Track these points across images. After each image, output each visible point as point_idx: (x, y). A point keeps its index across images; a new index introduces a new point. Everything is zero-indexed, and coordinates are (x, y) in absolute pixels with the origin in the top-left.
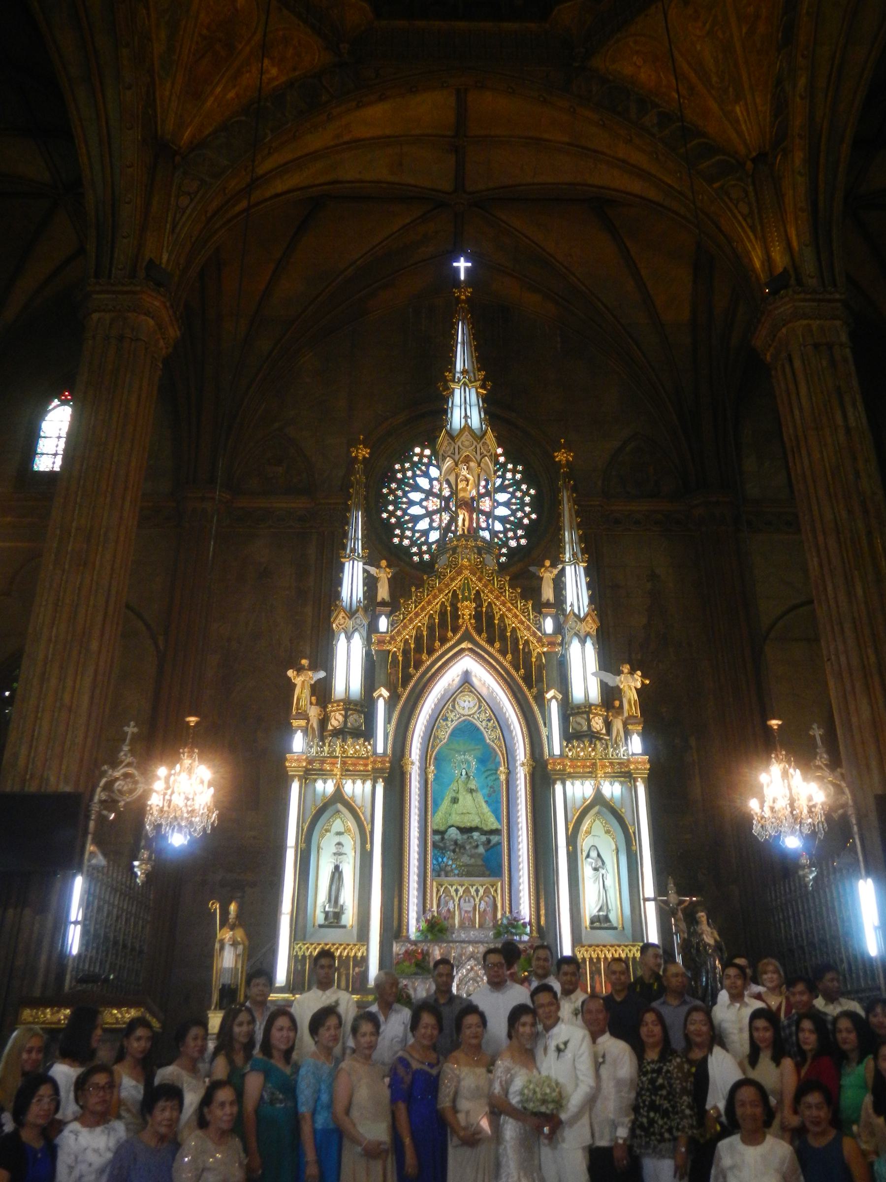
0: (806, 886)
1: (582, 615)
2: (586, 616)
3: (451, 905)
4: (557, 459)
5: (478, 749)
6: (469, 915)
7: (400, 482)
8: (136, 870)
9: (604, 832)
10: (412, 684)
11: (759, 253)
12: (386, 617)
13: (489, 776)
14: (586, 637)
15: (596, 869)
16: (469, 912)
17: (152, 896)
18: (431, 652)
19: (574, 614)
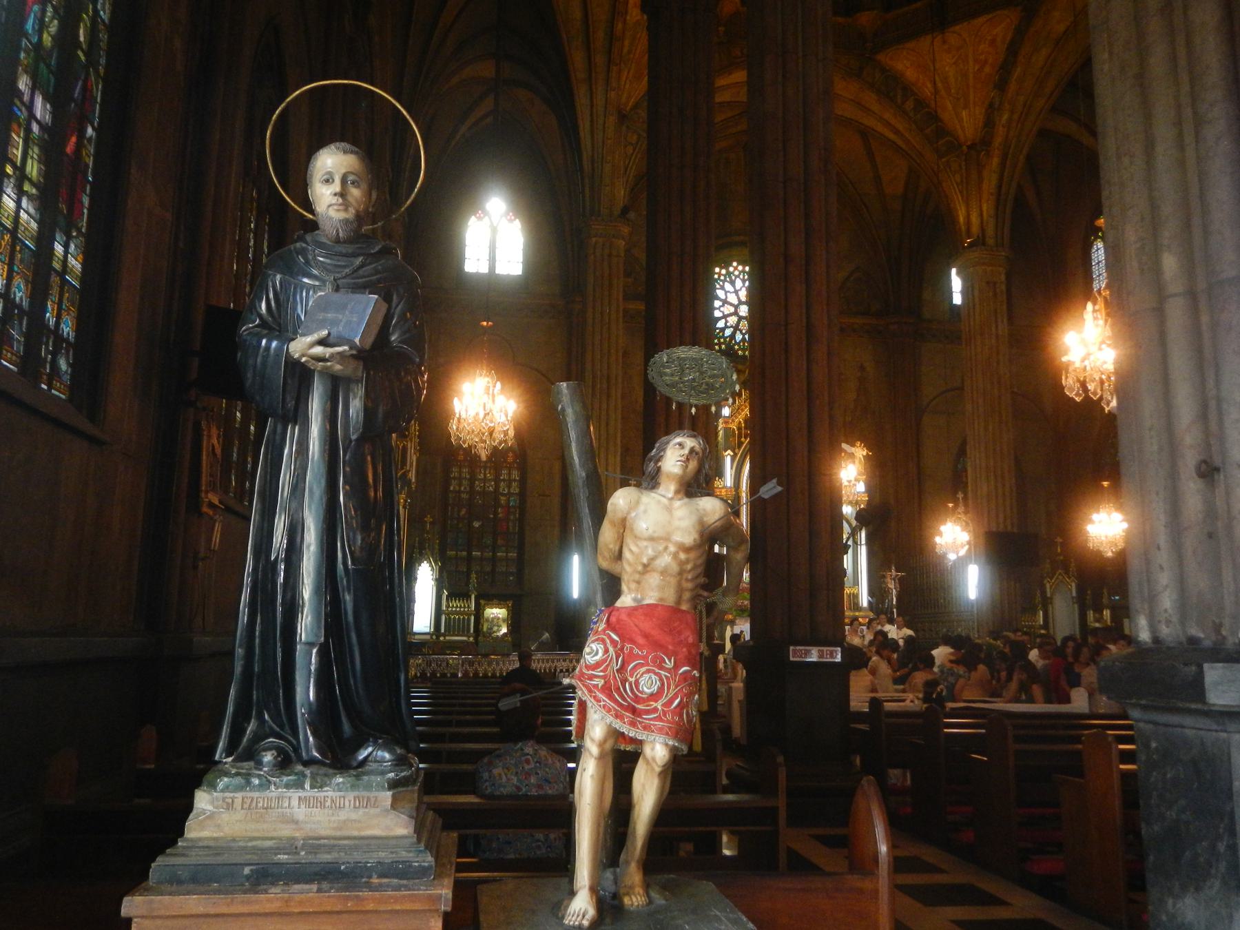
11: (964, 212)
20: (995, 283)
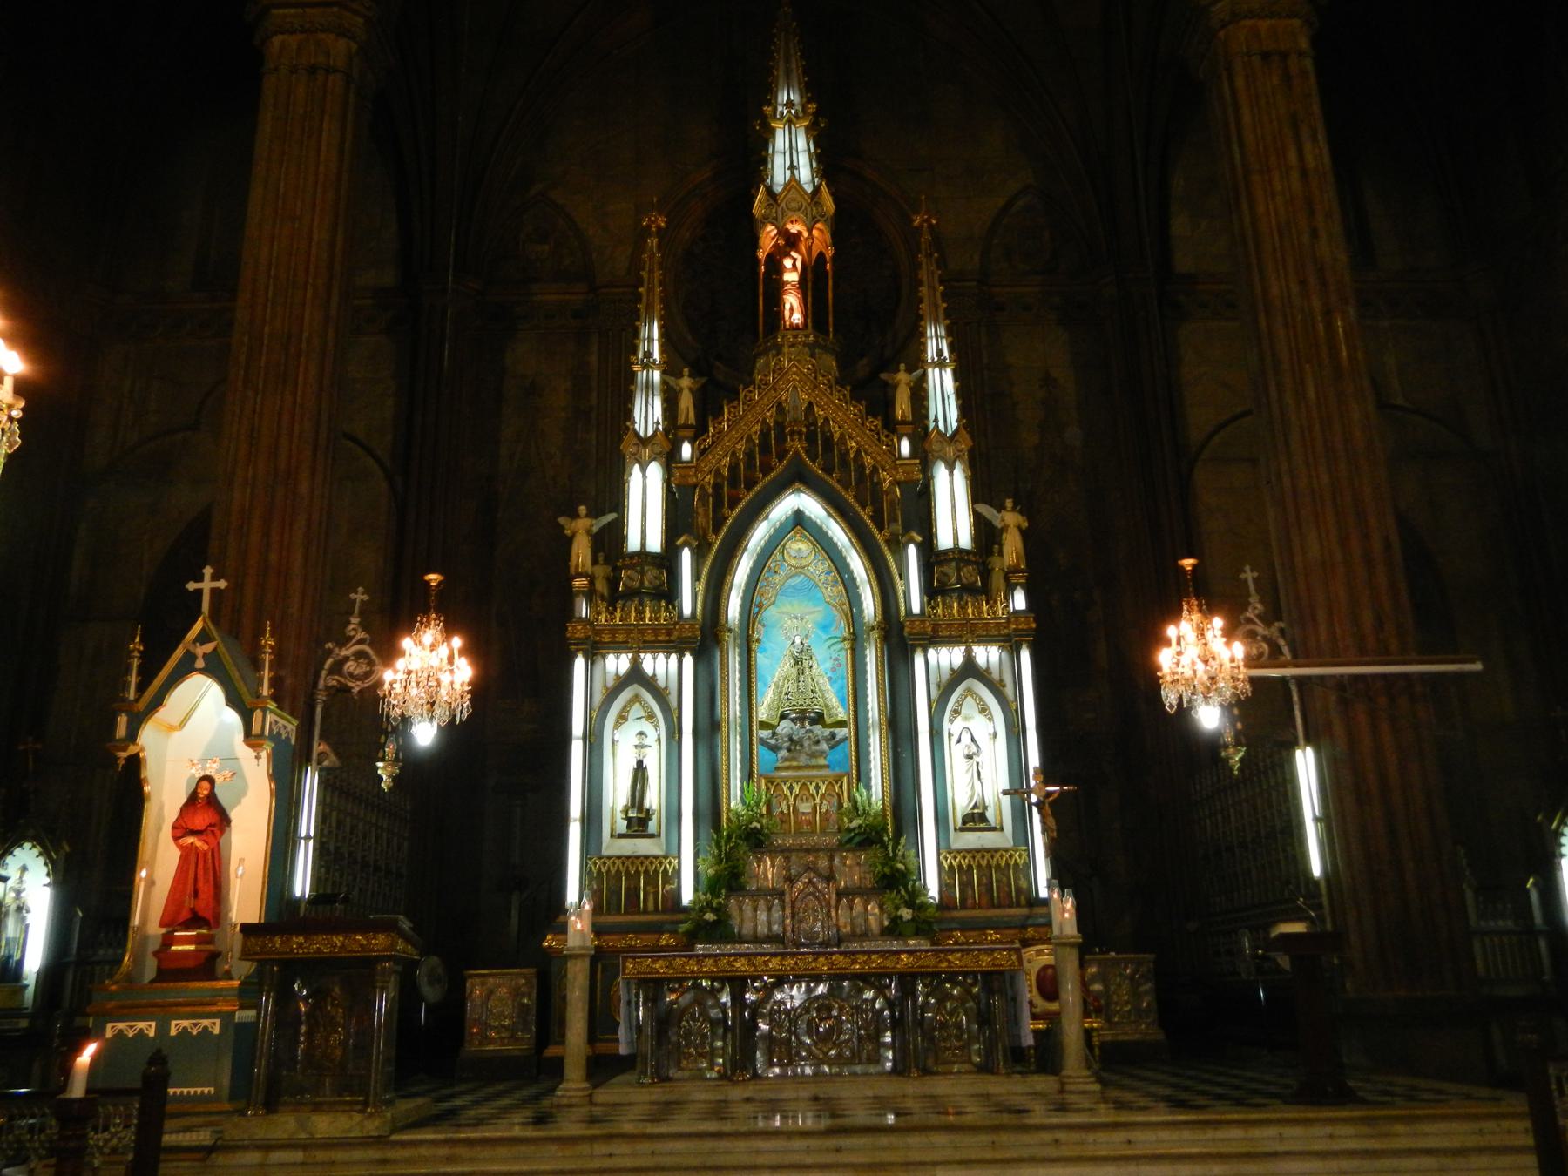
0: (1231, 770)
1: (949, 433)
2: (956, 433)
3: (784, 805)
4: (916, 223)
5: (819, 611)
6: (808, 818)
8: (379, 772)
9: (977, 711)
10: (725, 528)
12: (689, 442)
13: (833, 644)
14: (955, 461)
15: (970, 757)
16: (809, 813)
17: (408, 807)
18: (750, 485)
19: (939, 432)
20: (1284, 56)
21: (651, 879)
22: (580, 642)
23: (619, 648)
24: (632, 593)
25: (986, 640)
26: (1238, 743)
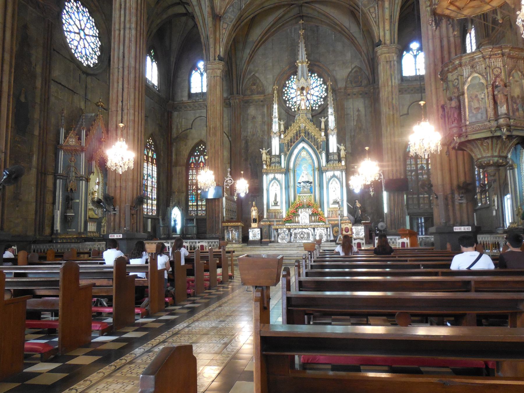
7: (288, 87)
18: (294, 143)
21: (278, 213)
22: (265, 173)
23: (271, 173)
24: (273, 163)
25: (337, 170)
26: (373, 192)
